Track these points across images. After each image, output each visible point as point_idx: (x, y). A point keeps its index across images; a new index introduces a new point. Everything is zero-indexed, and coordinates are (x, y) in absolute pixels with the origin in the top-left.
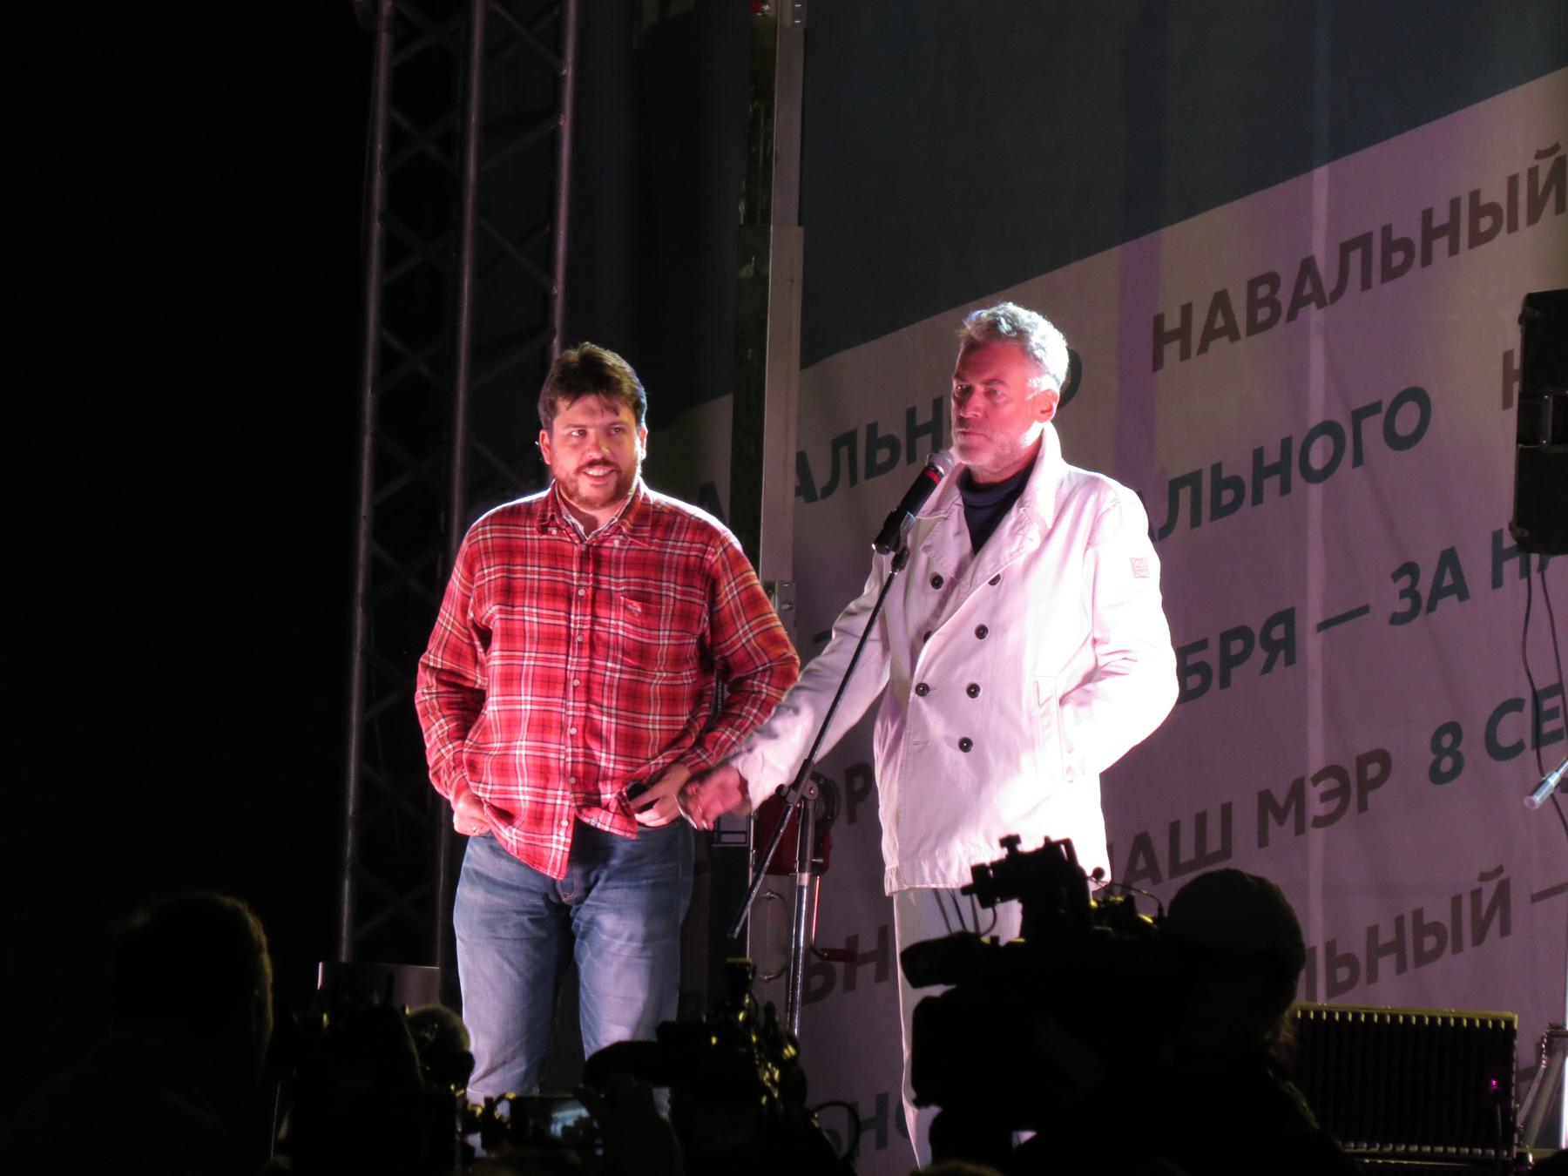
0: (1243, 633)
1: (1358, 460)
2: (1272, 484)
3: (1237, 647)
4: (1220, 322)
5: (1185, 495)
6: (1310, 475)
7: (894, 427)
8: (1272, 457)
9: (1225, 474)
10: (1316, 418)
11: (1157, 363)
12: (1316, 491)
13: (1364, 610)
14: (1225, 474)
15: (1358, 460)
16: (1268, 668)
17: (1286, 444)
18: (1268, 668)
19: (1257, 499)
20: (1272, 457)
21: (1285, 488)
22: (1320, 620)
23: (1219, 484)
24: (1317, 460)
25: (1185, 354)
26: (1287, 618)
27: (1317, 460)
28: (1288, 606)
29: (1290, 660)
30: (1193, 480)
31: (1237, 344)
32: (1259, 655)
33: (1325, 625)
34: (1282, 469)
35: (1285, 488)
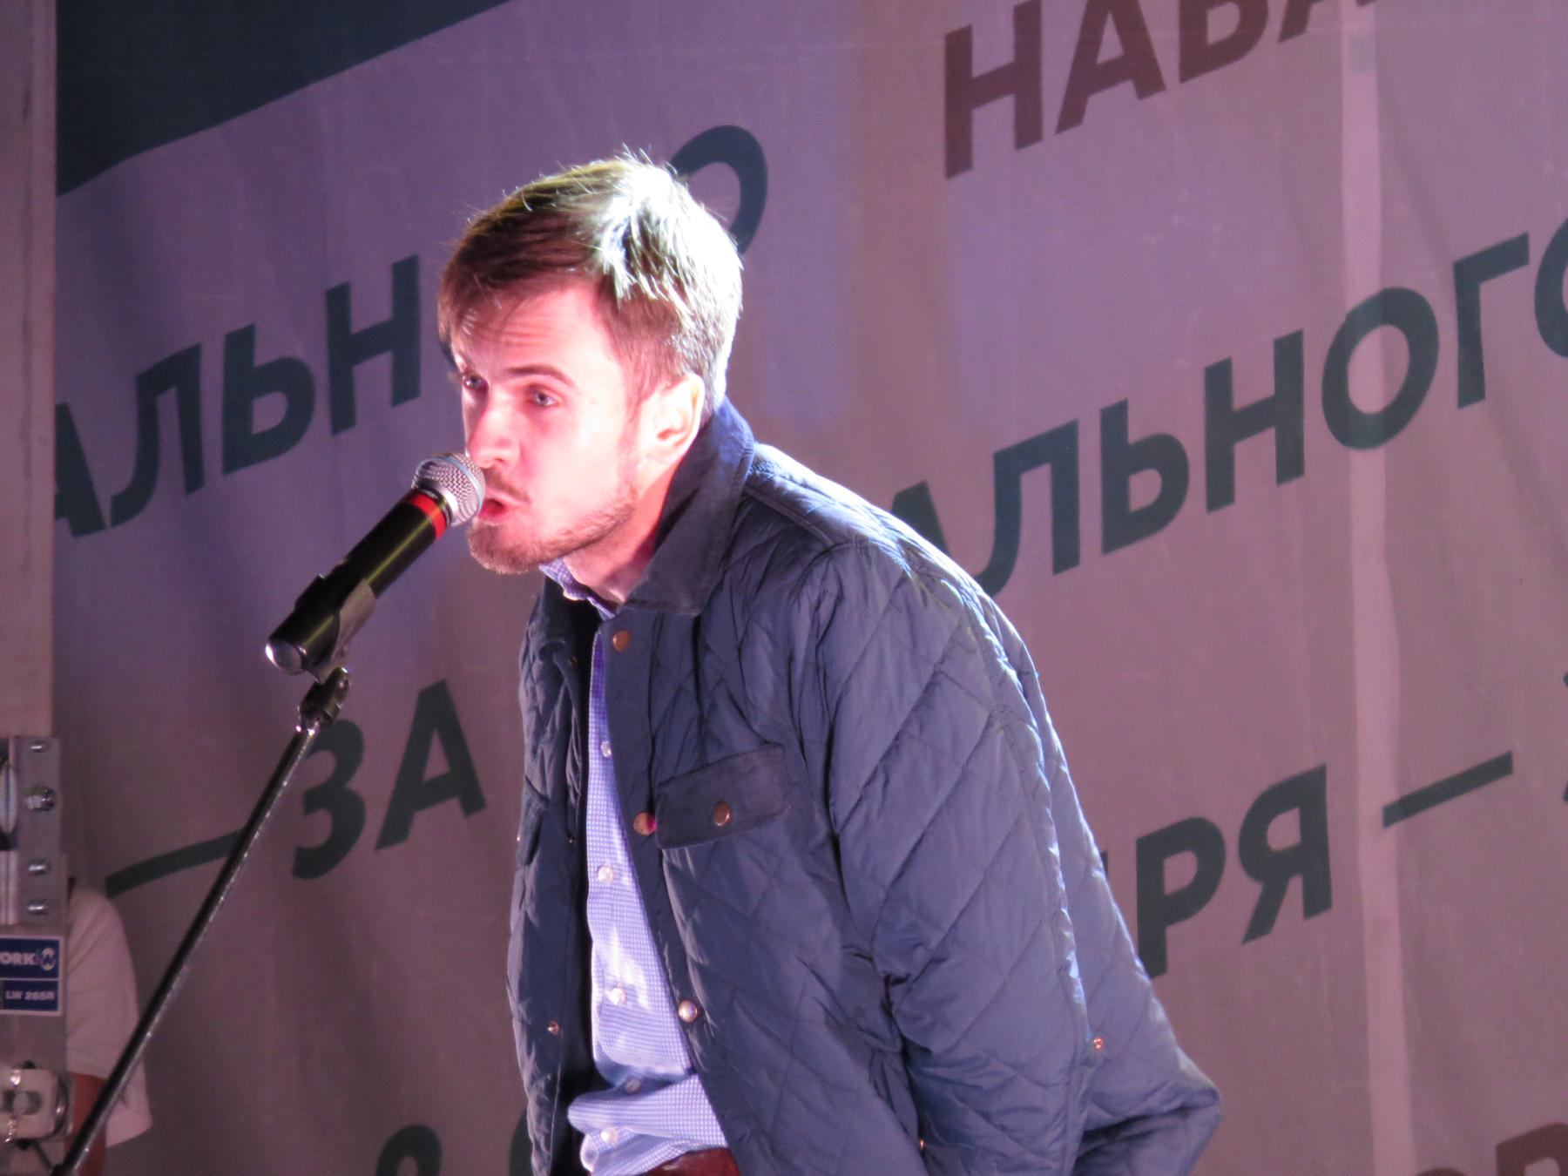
0: (1196, 835)
1: (1472, 386)
2: (1255, 455)
3: (1180, 870)
4: (1111, 46)
5: (1036, 486)
6: (1348, 426)
7: (293, 337)
8: (1254, 383)
9: (1136, 432)
10: (1362, 285)
11: (958, 157)
12: (1367, 469)
13: (1501, 767)
14: (1136, 432)
15: (1472, 386)
16: (1262, 922)
17: (1289, 352)
18: (1262, 922)
19: (1220, 492)
20: (1254, 383)
21: (1290, 465)
22: (1391, 795)
23: (1122, 458)
24: (1369, 388)
25: (1027, 131)
26: (1305, 793)
27: (1369, 388)
28: (1304, 763)
29: (1317, 901)
30: (1056, 449)
31: (1156, 100)
32: (1238, 891)
33: (1404, 808)
34: (1280, 413)
35: (1290, 465)
